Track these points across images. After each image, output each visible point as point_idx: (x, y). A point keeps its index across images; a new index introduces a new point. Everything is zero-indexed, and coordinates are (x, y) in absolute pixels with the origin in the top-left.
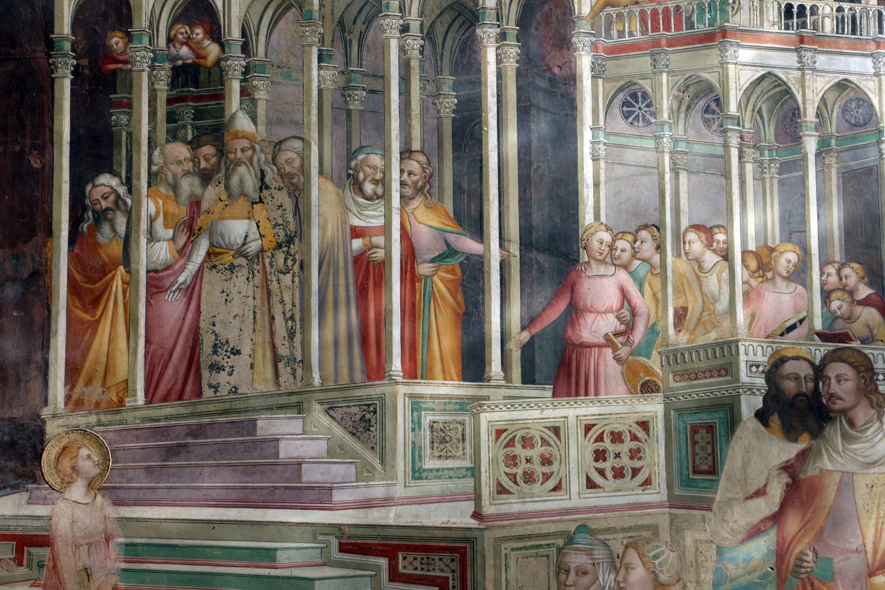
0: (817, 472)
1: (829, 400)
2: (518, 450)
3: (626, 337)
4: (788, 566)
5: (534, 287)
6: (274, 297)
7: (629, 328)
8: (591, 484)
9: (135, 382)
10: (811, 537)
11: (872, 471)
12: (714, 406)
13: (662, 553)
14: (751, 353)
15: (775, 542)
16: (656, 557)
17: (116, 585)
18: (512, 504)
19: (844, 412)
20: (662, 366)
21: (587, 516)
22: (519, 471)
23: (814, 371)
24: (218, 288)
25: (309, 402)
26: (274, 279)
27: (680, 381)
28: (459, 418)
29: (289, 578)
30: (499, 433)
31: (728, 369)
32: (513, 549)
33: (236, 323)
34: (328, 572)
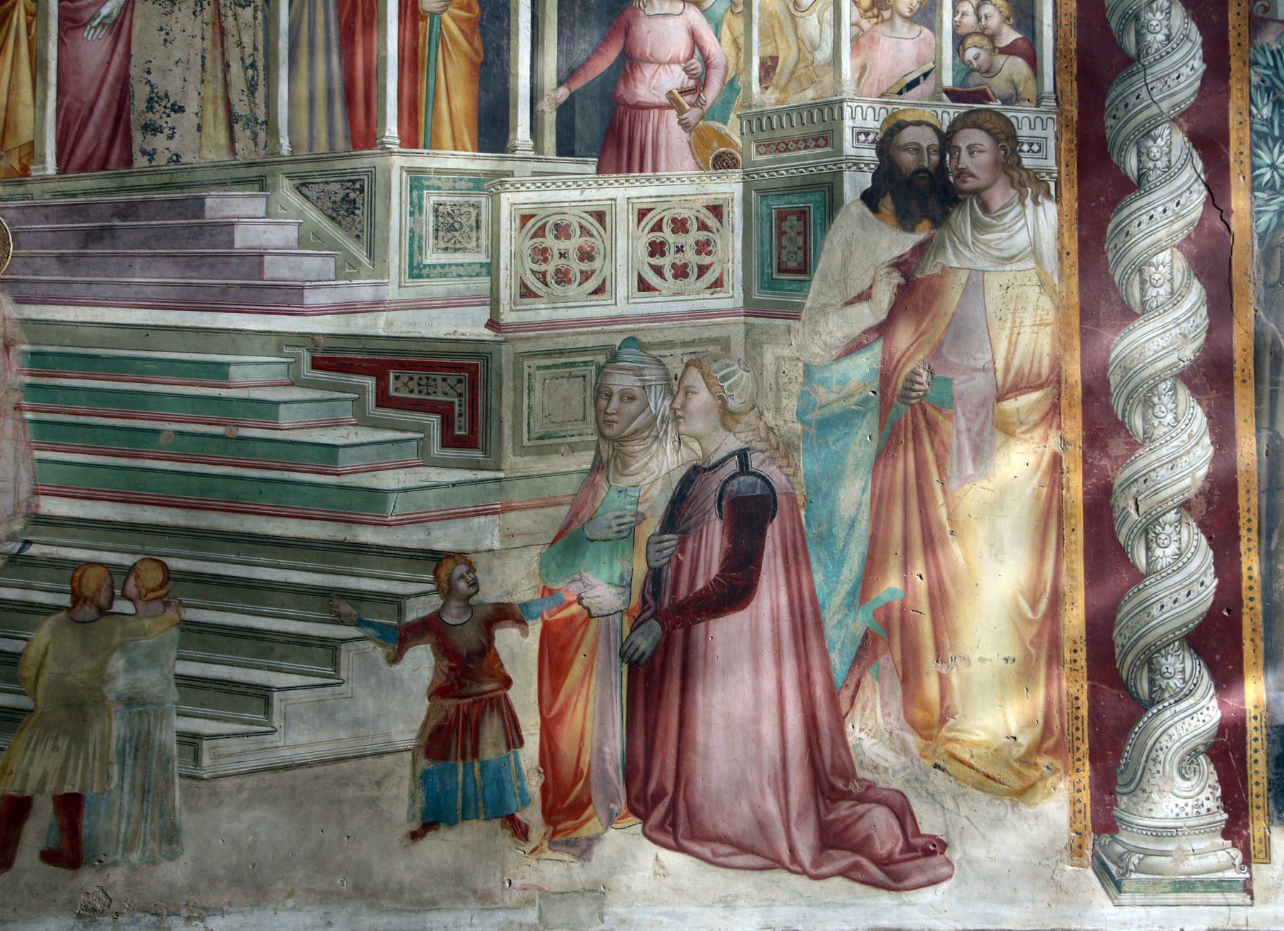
0: (938, 270)
1: (957, 177)
2: (549, 241)
3: (696, 95)
4: (894, 389)
5: (576, 30)
6: (230, 38)
7: (701, 83)
8: (644, 286)
9: (43, 145)
10: (927, 352)
11: (1008, 268)
12: (808, 186)
13: (734, 373)
14: (859, 117)
15: (879, 359)
16: (724, 378)
17: (18, 404)
18: (541, 312)
19: (976, 192)
20: (743, 134)
21: (638, 326)
22: (550, 268)
23: (940, 140)
24: (155, 24)
25: (275, 176)
26: (230, 13)
27: (765, 153)
28: (473, 200)
29: (245, 400)
30: (525, 219)
31: (828, 137)
32: (539, 368)
33: (178, 70)
34: (296, 393)
